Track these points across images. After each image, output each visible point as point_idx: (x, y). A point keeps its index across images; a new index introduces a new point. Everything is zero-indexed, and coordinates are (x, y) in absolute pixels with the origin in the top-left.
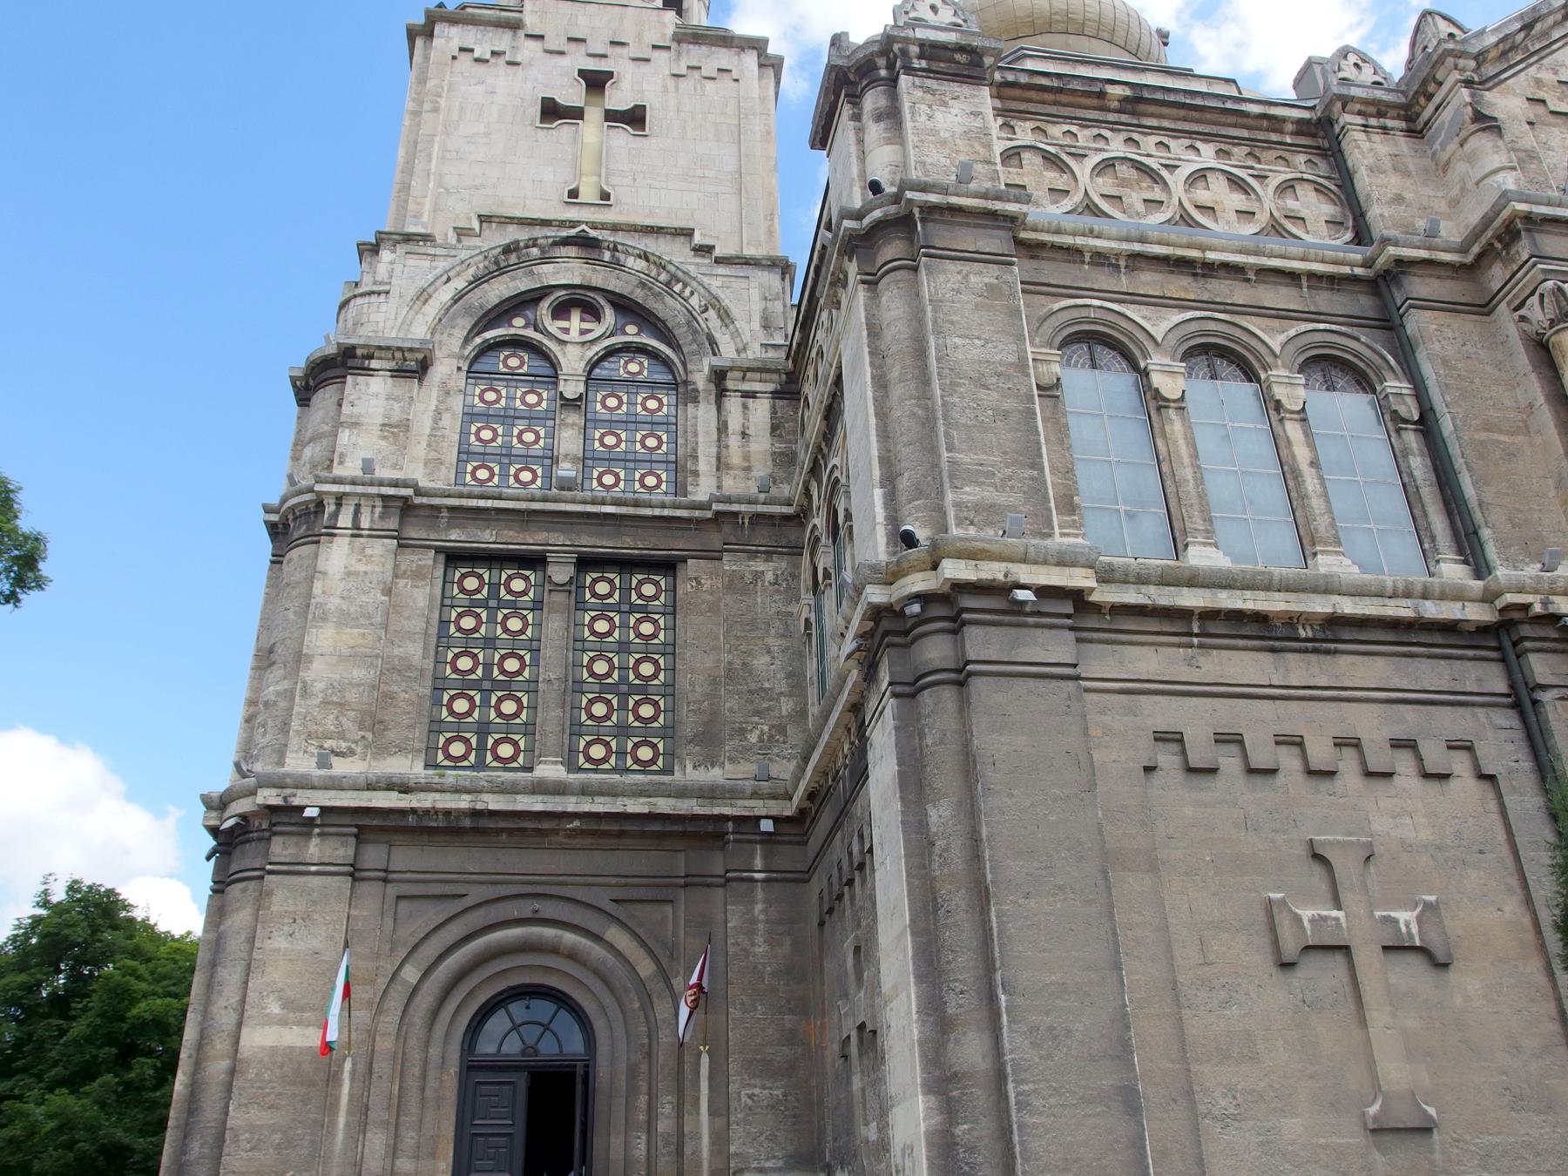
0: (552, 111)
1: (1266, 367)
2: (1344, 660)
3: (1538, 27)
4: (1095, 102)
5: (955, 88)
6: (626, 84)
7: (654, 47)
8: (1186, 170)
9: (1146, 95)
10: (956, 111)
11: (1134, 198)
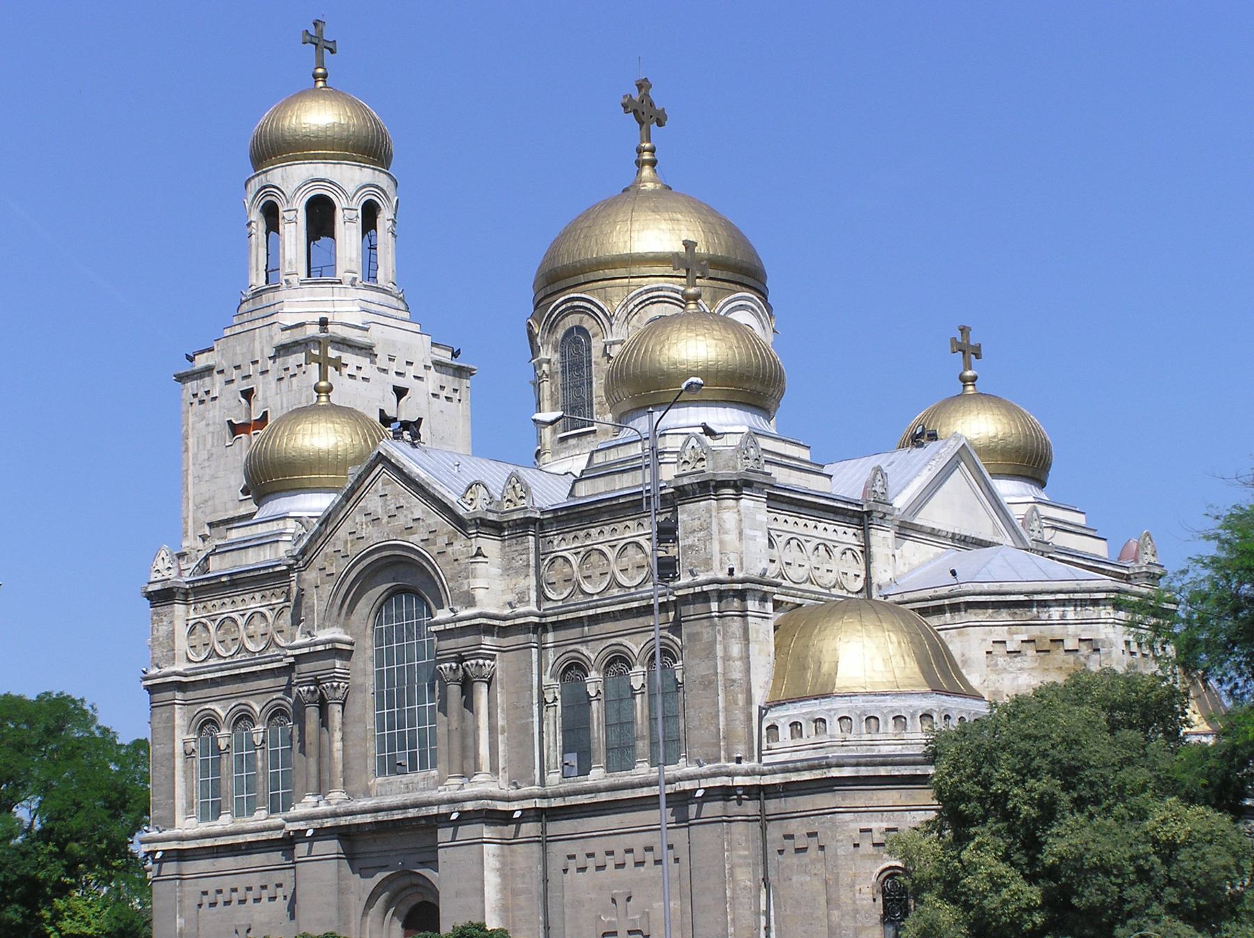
0: (235, 429)
4: (221, 585)
6: (260, 396)
7: (270, 358)
8: (246, 617)
9: (235, 577)
10: (165, 623)
11: (229, 641)
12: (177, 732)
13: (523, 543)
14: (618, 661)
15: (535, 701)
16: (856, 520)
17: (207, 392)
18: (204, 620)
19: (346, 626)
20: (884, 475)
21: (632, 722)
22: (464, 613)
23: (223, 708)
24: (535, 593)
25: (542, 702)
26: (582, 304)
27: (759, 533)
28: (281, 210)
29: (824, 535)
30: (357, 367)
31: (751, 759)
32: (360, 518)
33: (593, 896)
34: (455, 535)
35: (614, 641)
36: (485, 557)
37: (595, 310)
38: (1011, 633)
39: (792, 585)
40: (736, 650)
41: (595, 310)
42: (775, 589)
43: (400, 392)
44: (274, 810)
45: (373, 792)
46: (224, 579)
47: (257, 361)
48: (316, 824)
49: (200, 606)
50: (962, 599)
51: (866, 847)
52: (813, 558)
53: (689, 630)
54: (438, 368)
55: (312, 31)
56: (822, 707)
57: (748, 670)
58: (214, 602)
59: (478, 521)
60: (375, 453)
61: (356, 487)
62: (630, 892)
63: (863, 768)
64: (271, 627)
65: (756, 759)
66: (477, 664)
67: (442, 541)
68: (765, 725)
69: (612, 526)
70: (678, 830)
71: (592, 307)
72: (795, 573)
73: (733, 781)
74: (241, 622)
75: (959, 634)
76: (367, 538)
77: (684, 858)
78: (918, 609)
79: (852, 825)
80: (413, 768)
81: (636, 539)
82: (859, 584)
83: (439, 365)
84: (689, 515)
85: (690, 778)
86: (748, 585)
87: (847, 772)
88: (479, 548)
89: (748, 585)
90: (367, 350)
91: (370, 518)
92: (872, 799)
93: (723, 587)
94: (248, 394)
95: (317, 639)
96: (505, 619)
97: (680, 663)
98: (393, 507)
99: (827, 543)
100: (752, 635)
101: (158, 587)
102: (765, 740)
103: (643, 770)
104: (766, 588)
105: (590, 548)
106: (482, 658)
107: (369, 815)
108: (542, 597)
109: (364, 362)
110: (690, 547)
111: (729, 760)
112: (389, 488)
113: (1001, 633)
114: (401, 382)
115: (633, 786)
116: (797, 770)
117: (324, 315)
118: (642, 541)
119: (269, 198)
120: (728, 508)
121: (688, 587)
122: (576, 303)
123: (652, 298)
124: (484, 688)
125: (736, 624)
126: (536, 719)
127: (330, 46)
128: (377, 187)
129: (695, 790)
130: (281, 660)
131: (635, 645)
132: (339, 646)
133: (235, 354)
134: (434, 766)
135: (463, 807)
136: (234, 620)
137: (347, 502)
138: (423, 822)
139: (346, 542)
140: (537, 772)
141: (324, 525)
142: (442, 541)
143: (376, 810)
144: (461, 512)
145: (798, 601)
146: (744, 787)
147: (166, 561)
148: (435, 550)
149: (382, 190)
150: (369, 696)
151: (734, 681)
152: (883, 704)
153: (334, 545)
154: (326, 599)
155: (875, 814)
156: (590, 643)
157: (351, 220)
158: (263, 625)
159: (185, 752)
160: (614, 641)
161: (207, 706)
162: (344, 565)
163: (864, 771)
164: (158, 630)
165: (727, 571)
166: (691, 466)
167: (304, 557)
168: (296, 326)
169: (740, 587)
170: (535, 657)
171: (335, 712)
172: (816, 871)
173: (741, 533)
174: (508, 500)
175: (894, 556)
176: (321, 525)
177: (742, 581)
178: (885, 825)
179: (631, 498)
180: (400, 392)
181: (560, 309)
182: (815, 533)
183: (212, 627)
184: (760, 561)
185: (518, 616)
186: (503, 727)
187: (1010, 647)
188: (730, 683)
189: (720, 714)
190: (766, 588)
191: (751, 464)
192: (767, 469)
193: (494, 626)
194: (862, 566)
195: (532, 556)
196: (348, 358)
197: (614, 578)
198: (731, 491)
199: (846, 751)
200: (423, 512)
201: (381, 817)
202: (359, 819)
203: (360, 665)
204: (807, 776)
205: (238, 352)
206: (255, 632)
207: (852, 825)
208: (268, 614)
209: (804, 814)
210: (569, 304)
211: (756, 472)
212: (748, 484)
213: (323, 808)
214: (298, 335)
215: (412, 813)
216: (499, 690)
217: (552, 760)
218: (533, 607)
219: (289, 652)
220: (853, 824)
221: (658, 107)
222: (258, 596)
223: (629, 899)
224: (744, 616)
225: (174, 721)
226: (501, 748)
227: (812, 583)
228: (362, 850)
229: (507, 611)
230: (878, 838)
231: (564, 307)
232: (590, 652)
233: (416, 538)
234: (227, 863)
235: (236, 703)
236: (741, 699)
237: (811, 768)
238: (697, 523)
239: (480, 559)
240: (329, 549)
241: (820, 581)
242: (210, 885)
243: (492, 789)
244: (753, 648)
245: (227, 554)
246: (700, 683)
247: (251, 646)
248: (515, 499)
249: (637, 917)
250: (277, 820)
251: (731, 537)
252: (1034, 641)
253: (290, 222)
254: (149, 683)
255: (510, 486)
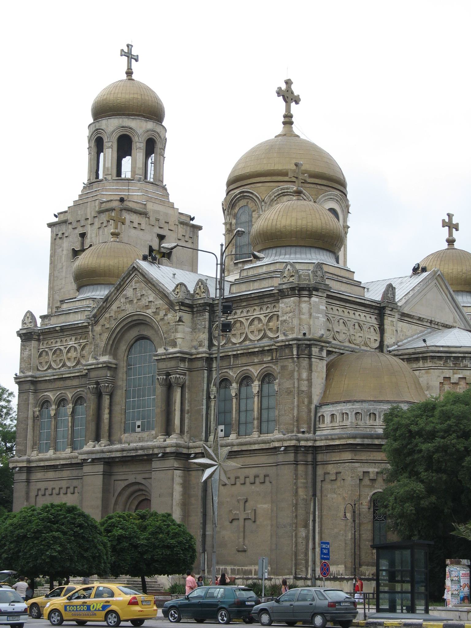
1: (70, 403)
2: (64, 472)
3: (110, 298)
4: (55, 332)
5: (28, 343)
8: (67, 349)
10: (27, 350)
11: (58, 361)
12: (30, 406)
13: (203, 316)
14: (246, 380)
15: (205, 397)
16: (377, 311)
17: (63, 234)
18: (46, 349)
19: (115, 356)
20: (394, 289)
21: (253, 410)
22: (171, 350)
23: (54, 395)
24: (208, 342)
25: (208, 398)
26: (248, 194)
27: (320, 315)
28: (105, 141)
29: (358, 318)
30: (138, 224)
31: (309, 432)
32: (123, 300)
33: (228, 500)
34: (169, 310)
35: (245, 368)
36: (183, 322)
37: (255, 198)
38: (454, 374)
39: (339, 343)
40: (304, 375)
41: (255, 198)
42: (327, 345)
43: (161, 238)
44: (74, 449)
45: (123, 441)
46: (57, 329)
47: (88, 218)
48: (94, 456)
49: (46, 342)
50: (428, 355)
51: (366, 481)
52: (351, 330)
53: (282, 364)
54: (182, 226)
55: (126, 50)
56: (347, 407)
57: (310, 386)
58: (52, 340)
59: (180, 303)
60: (132, 266)
61: (122, 283)
62: (247, 499)
63: (366, 440)
64: (79, 355)
65: (312, 432)
66: (176, 377)
67: (162, 313)
68: (319, 414)
69: (248, 309)
70: (271, 467)
71: (253, 196)
72: (341, 337)
73: (299, 443)
74: (65, 351)
75: (426, 373)
76: (126, 310)
77: (274, 482)
78: (407, 359)
79: (359, 469)
80: (143, 430)
81: (259, 316)
82: (377, 345)
83: (182, 223)
84: (285, 305)
85: (279, 440)
86: (312, 342)
87: (358, 441)
88: (180, 317)
89: (312, 342)
90: (144, 214)
91: (127, 300)
92: (370, 456)
93: (300, 342)
94: (83, 235)
95: (99, 361)
96: (192, 355)
97: (277, 381)
98: (139, 295)
99: (361, 322)
100: (314, 368)
101: (24, 331)
102: (318, 423)
103: (255, 436)
104: (323, 344)
105: (236, 320)
106: (179, 374)
107: (119, 453)
108: (211, 345)
109: (143, 220)
110: (285, 321)
111: (299, 432)
112: (138, 285)
113: (448, 373)
114: (162, 232)
115: (250, 444)
116: (333, 439)
117: (123, 196)
118: (262, 317)
119: (99, 135)
120: (305, 302)
121: (282, 341)
122: (245, 194)
123: (284, 192)
124: (179, 390)
125: (305, 363)
126: (204, 407)
127: (136, 57)
128: (155, 131)
129: (280, 447)
130: (82, 372)
131: (255, 371)
132: (110, 365)
133: (77, 215)
134: (153, 429)
135: (165, 450)
136: (60, 350)
137: (118, 291)
138: (145, 457)
139: (115, 312)
140: (204, 434)
141: (105, 303)
142: (162, 313)
143: (123, 450)
144: (172, 298)
145: (342, 351)
146: (305, 446)
147: (30, 318)
148: (159, 318)
149: (158, 133)
150: (124, 392)
151: (303, 391)
152: (379, 407)
153: (110, 313)
154: (104, 341)
155: (371, 464)
156: (234, 369)
157: (140, 148)
158: (75, 353)
159: (34, 416)
160: (245, 368)
161: (46, 394)
162: (113, 324)
163: (367, 441)
164: (23, 354)
165: (302, 334)
166: (287, 279)
167: (96, 319)
168: (108, 201)
169: (308, 343)
170: (206, 375)
171: (106, 401)
172: (339, 492)
173: (311, 315)
174: (197, 293)
175: (397, 331)
176: (104, 303)
177: (309, 340)
178: (376, 470)
179: (258, 295)
180: (161, 238)
181: (238, 197)
182: (353, 316)
183: (50, 354)
184: (321, 330)
185: (198, 354)
186: (188, 410)
187: (452, 381)
188: (300, 392)
189: (295, 408)
190: (323, 344)
191: (319, 279)
192: (328, 282)
193: (186, 358)
194: (379, 335)
195: (207, 323)
196: (136, 218)
197: (247, 336)
198: (306, 293)
199: (358, 430)
200: (154, 298)
201: (125, 454)
202: (113, 455)
203: (120, 375)
204: (337, 442)
205: (79, 214)
206: (71, 356)
207: (359, 469)
208: (78, 347)
209: (335, 462)
210: (242, 195)
211: (321, 284)
212: (317, 290)
213: (97, 448)
214: (109, 205)
215: (140, 452)
216: (187, 391)
217: (212, 428)
218: (205, 349)
219: (85, 368)
220: (361, 469)
221: (296, 94)
222: (73, 338)
223: (246, 501)
224: (310, 358)
225: (29, 400)
226: (186, 421)
227: (350, 342)
228: (116, 471)
229: (194, 351)
230: (372, 476)
231: (239, 196)
232: (232, 374)
233: (149, 311)
234: (51, 475)
235: (60, 392)
236: (306, 400)
237: (339, 439)
238: (289, 308)
239: (181, 323)
240: (107, 315)
241: (355, 342)
242: (42, 485)
243: (181, 442)
244: (314, 375)
245: (60, 316)
246: (286, 392)
247: (69, 364)
248: (200, 293)
249: (250, 511)
250: (75, 454)
251: (305, 317)
252: (465, 378)
253: (109, 148)
254: (18, 380)
255: (198, 286)
